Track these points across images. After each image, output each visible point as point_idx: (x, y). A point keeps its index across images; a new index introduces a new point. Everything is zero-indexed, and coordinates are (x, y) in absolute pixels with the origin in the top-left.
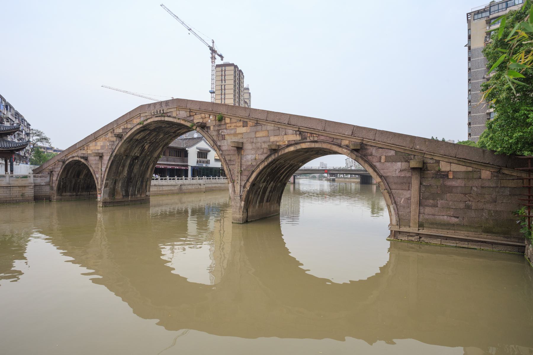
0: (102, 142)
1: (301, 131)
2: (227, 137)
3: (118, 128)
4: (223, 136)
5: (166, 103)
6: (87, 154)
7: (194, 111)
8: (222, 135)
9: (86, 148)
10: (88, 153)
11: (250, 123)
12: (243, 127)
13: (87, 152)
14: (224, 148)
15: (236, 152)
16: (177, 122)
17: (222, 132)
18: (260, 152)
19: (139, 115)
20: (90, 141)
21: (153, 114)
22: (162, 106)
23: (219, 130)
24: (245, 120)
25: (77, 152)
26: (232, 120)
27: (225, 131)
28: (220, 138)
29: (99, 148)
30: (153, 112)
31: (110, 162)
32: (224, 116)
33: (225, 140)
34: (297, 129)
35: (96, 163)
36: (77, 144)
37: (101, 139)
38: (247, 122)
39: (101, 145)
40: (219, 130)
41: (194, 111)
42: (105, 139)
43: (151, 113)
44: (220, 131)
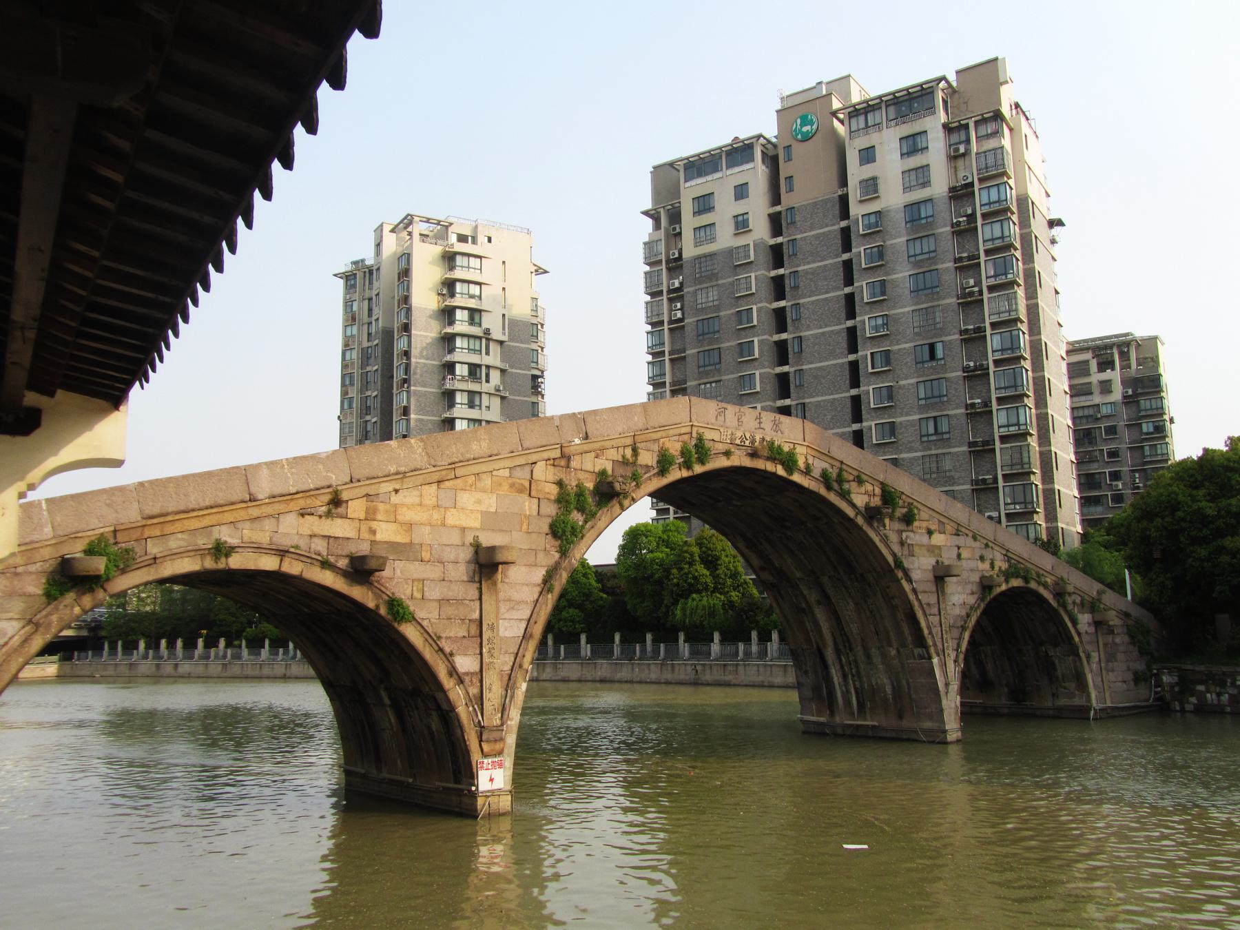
0: (494, 497)
1: (1012, 558)
2: (916, 549)
3: (593, 454)
4: (911, 548)
5: (775, 421)
6: (373, 543)
7: (849, 470)
8: (909, 545)
9: (356, 508)
10: (379, 537)
11: (948, 528)
12: (940, 533)
13: (373, 532)
14: (916, 575)
15: (934, 589)
16: (811, 488)
17: (907, 537)
18: (969, 588)
19: (688, 430)
20: (401, 475)
21: (738, 442)
22: (762, 426)
23: (902, 531)
24: (942, 519)
25: (268, 525)
26: (922, 513)
27: (911, 534)
28: (906, 552)
29: (474, 522)
30: (739, 434)
31: (550, 600)
32: (915, 503)
33: (913, 556)
34: (1004, 552)
35: (450, 595)
36: (265, 472)
37: (487, 481)
38: (943, 523)
39: (483, 508)
40: (902, 531)
41: (849, 470)
42: (512, 486)
43: (731, 439)
44: (904, 535)
